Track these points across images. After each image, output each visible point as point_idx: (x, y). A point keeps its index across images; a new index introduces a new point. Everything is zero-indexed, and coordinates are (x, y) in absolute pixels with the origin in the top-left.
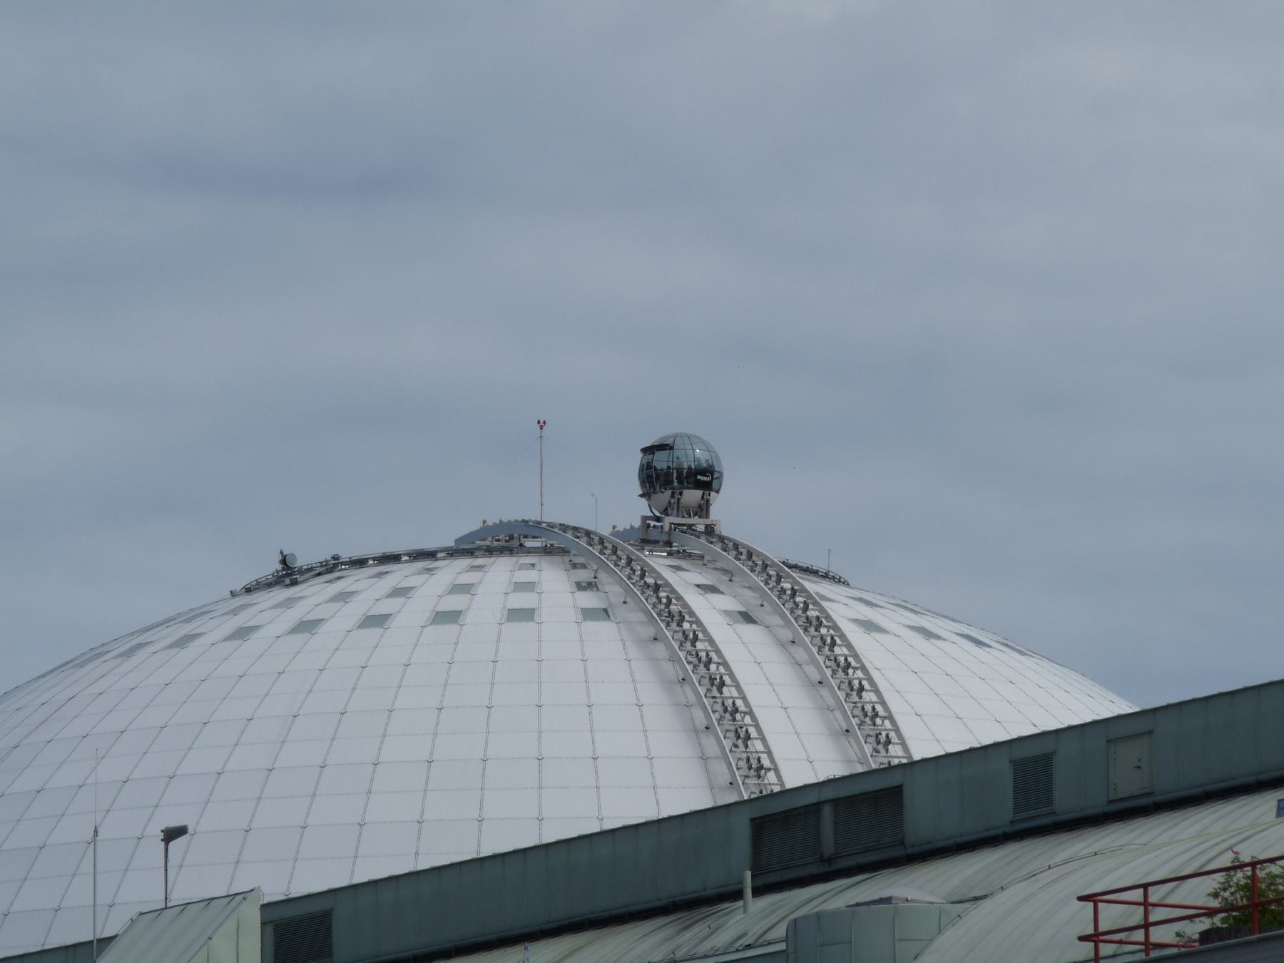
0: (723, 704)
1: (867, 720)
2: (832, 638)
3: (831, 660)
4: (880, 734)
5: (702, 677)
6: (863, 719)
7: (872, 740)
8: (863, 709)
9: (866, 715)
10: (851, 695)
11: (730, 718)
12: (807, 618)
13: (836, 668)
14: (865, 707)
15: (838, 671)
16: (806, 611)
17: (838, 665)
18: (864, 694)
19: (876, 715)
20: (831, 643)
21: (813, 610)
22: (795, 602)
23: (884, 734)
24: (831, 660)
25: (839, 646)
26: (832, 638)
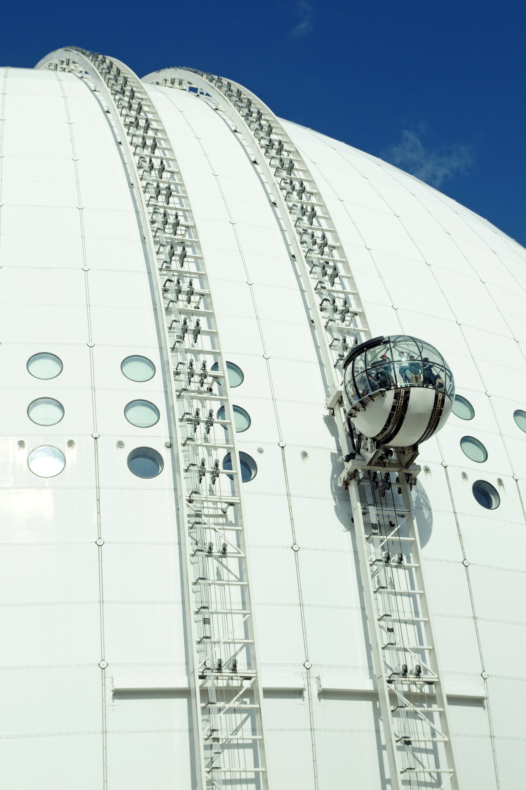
0: (165, 215)
1: (316, 247)
2: (291, 162)
3: (287, 183)
4: (327, 263)
5: (148, 184)
6: (311, 247)
7: (318, 270)
8: (313, 236)
9: (315, 243)
10: (302, 219)
11: (172, 231)
12: (270, 141)
13: (291, 191)
14: (315, 234)
15: (292, 193)
16: (269, 134)
17: (293, 188)
18: (314, 220)
19: (326, 244)
20: (289, 167)
21: (276, 134)
22: (260, 124)
23: (331, 264)
24: (287, 183)
25: (297, 170)
26: (291, 162)
